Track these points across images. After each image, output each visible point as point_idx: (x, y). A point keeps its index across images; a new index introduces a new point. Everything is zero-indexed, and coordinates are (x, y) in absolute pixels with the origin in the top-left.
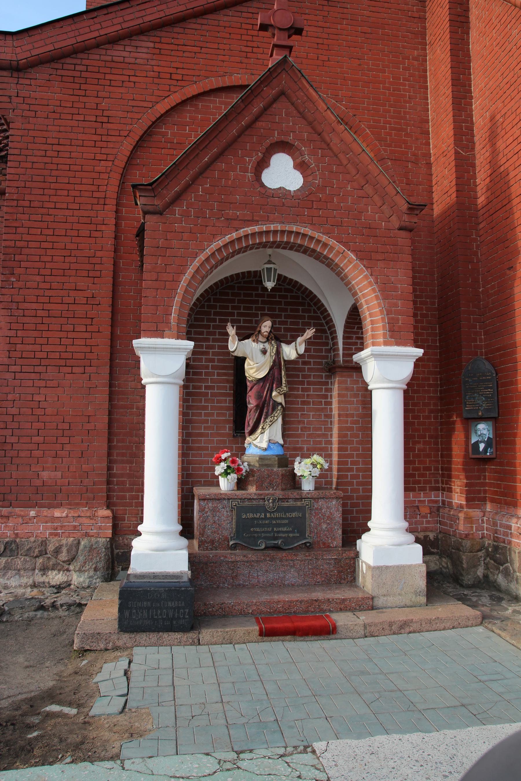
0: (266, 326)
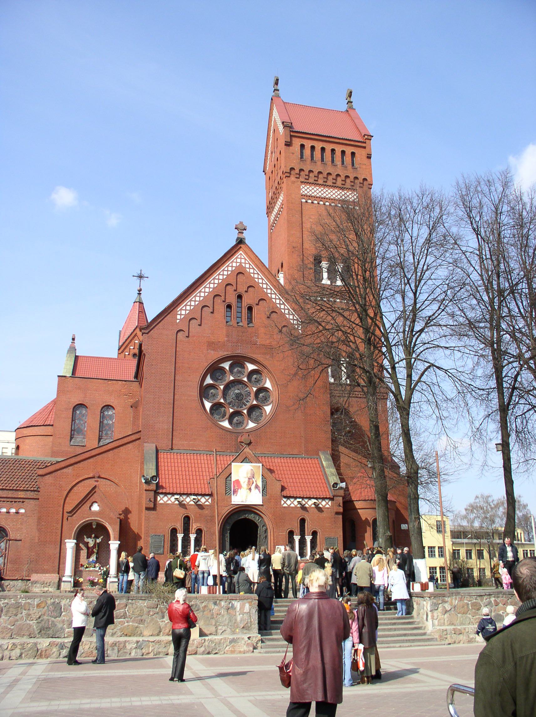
0: (93, 536)
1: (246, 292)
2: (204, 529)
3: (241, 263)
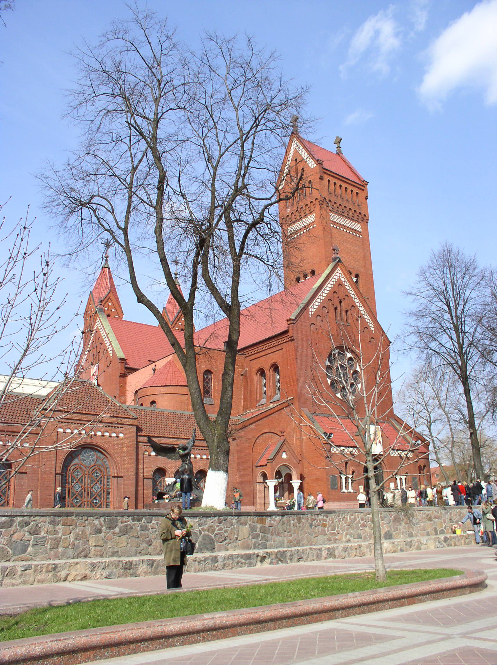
1: (344, 299)
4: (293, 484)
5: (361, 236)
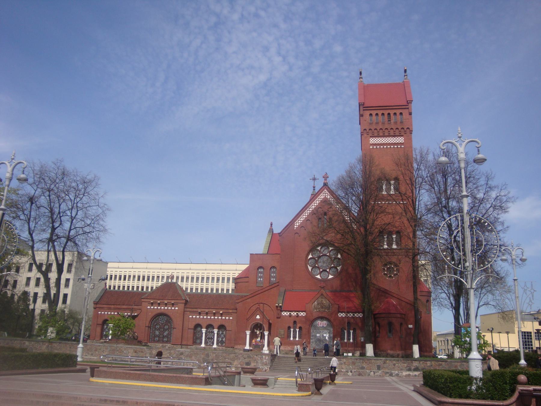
2: (303, 327)
3: (325, 196)
4: (265, 334)
5: (402, 146)
